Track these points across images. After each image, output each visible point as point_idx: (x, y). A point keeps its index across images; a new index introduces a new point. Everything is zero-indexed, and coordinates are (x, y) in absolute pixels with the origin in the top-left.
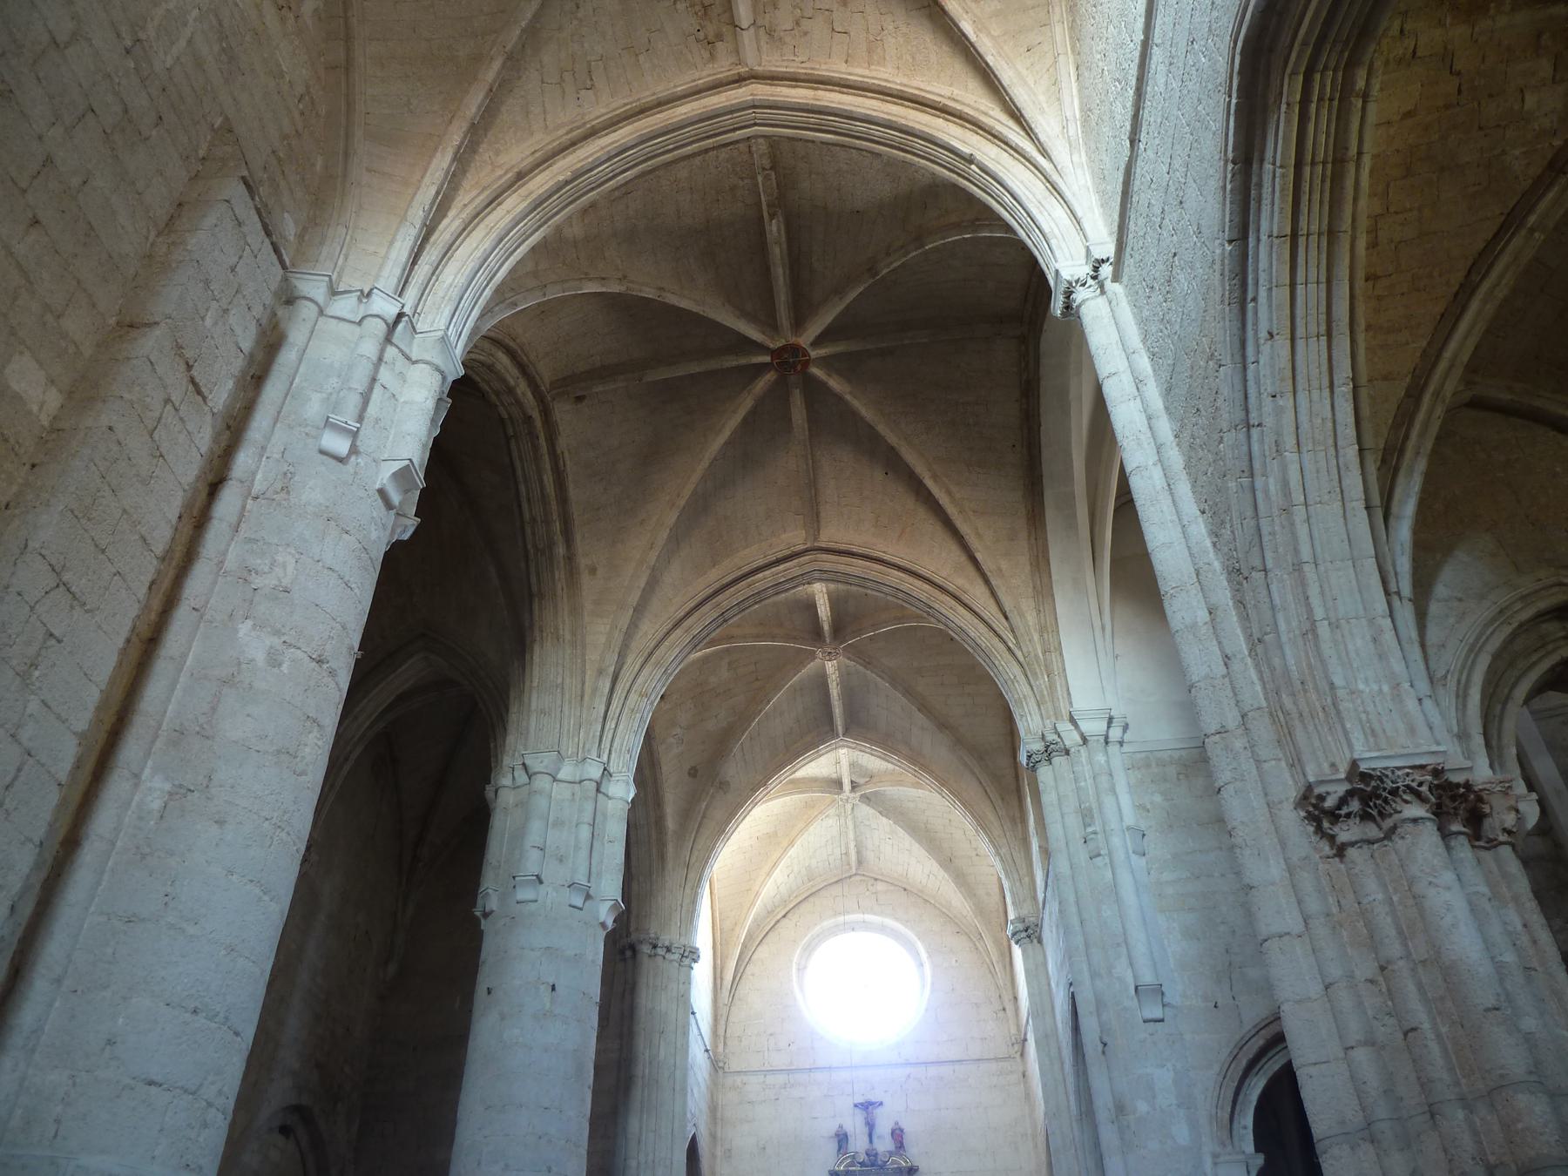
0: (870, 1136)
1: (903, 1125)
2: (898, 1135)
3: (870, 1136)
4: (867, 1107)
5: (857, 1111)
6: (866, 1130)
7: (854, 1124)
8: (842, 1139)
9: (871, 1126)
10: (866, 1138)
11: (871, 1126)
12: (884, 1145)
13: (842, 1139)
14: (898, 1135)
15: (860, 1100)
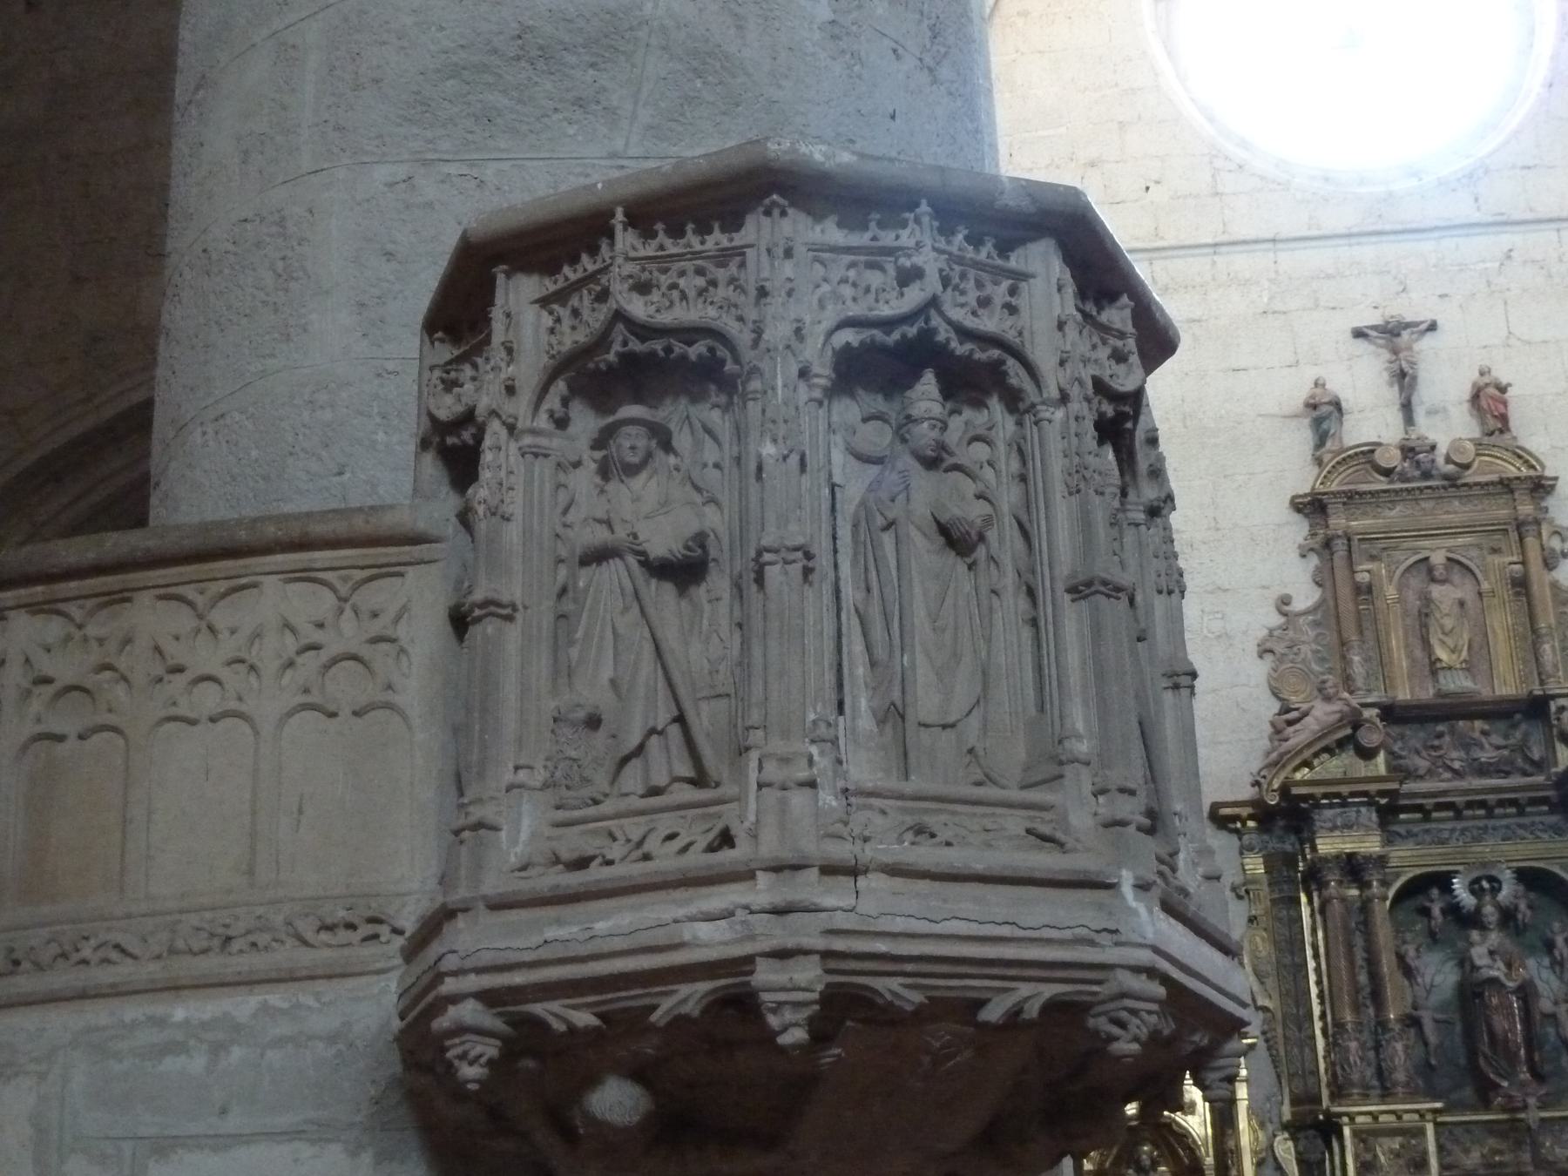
0: (1407, 408)
1: (1502, 374)
2: (1490, 403)
3: (1407, 408)
4: (1391, 335)
5: (1361, 344)
6: (1393, 394)
7: (1363, 386)
8: (1323, 413)
9: (1404, 379)
10: (1394, 417)
11: (1404, 379)
12: (1449, 428)
13: (1323, 413)
14: (1490, 403)
15: (1371, 318)
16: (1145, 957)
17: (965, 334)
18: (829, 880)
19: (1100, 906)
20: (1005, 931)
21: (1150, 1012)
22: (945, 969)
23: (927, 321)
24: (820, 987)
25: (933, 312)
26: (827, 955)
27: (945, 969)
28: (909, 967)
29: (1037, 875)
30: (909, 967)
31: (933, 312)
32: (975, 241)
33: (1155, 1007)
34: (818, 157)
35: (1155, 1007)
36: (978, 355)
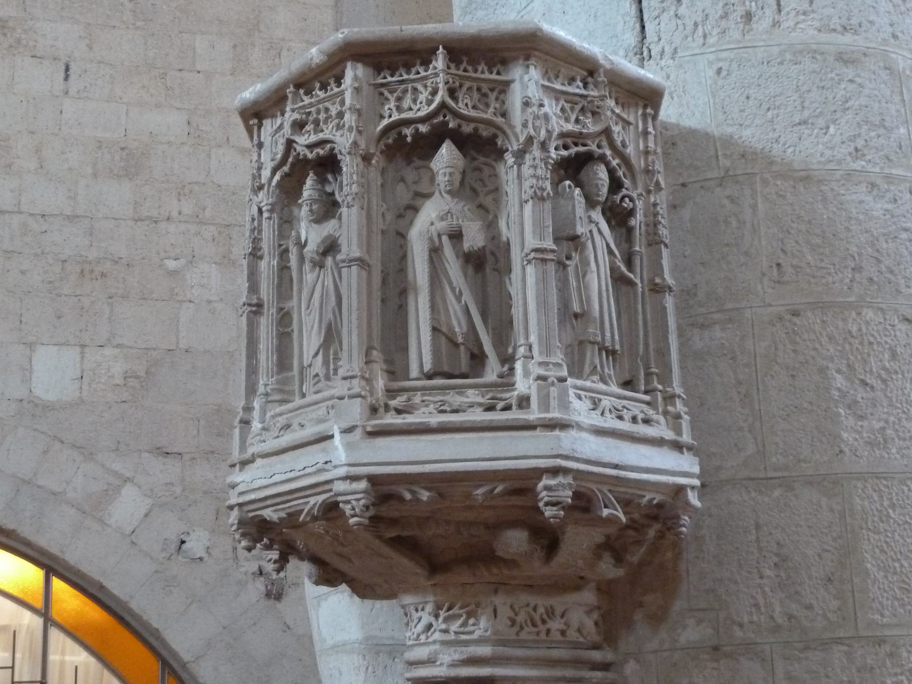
16: (342, 471)
17: (310, 147)
18: (247, 467)
19: (324, 450)
20: (291, 475)
21: (358, 500)
22: (278, 500)
23: (295, 150)
24: (236, 522)
25: (295, 145)
26: (240, 505)
27: (290, 497)
28: (269, 502)
29: (304, 441)
30: (269, 502)
31: (295, 145)
32: (324, 87)
33: (361, 496)
34: (248, 96)
35: (361, 496)
36: (321, 152)
